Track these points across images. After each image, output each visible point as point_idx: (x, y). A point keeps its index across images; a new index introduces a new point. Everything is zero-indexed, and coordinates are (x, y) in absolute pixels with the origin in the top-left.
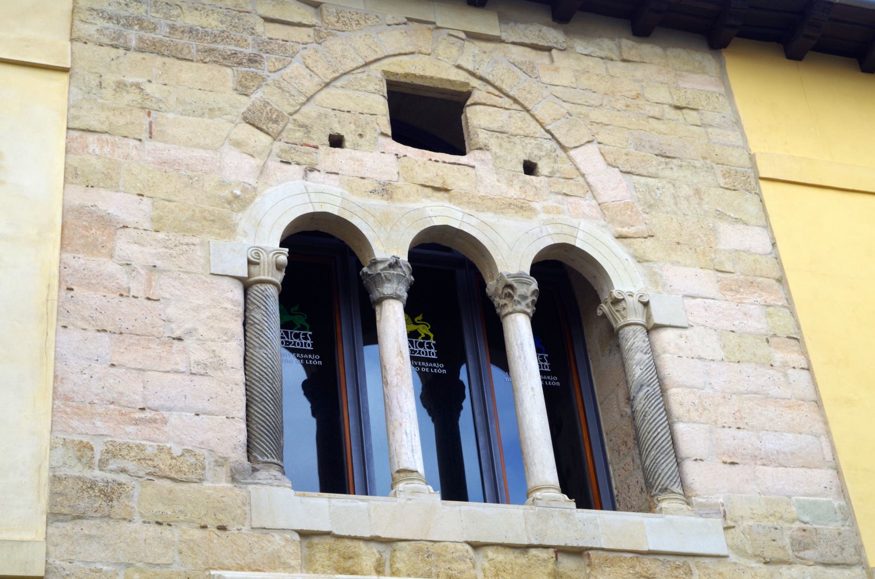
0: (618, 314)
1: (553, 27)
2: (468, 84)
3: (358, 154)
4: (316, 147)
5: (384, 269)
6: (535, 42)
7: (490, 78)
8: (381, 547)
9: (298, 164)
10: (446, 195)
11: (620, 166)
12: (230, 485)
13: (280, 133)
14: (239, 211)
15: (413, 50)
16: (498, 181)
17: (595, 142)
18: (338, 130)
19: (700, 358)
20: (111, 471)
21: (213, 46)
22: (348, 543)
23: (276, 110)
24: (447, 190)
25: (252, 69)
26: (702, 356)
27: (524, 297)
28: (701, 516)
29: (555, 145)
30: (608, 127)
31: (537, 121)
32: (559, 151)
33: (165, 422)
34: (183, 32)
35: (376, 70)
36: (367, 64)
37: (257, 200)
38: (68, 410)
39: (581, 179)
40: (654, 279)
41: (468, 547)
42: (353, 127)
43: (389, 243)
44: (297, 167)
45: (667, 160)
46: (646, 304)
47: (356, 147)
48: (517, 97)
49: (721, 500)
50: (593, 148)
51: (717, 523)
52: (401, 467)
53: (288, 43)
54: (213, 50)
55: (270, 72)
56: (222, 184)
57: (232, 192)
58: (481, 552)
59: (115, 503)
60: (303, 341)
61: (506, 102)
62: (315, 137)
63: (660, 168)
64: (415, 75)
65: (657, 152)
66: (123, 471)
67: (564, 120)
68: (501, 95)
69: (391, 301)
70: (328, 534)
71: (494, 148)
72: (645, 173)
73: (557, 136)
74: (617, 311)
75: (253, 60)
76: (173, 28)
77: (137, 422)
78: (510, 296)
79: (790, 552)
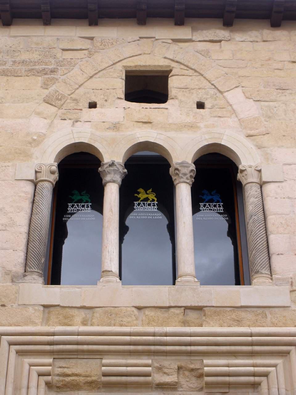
0: (243, 178)
1: (224, 29)
2: (170, 66)
3: (103, 110)
4: (81, 110)
5: (107, 168)
6: (212, 39)
7: (182, 61)
8: (87, 311)
9: (70, 119)
10: (150, 125)
11: (253, 98)
12: (11, 284)
13: (62, 105)
14: (35, 146)
15: (141, 53)
16: (181, 114)
17: (240, 87)
18: (94, 99)
19: (289, 198)
21: (33, 67)
22: (67, 310)
24: (150, 123)
25: (52, 76)
26: (290, 196)
27: (185, 174)
28: (277, 285)
30: (249, 78)
31: (207, 80)
32: (219, 94)
34: (19, 63)
35: (119, 66)
36: (114, 64)
37: (45, 140)
39: (230, 108)
41: (134, 309)
42: (102, 96)
43: (113, 155)
44: (70, 121)
45: (284, 91)
46: (260, 171)
47: (102, 106)
48: (196, 69)
49: (291, 276)
50: (239, 90)
51: (288, 288)
52: (104, 270)
53: (73, 60)
54: (33, 69)
55: (61, 76)
56: (28, 134)
57: (32, 138)
58: (143, 311)
60: (218, 208)
61: (190, 72)
62: (81, 104)
63: (279, 96)
64: (141, 66)
65: (277, 88)
67: (222, 77)
68: (188, 69)
69: (110, 184)
70: (58, 306)
71: (180, 98)
72: (268, 100)
73: (217, 86)
74: (243, 176)
75: (53, 71)
76: (14, 62)
78: (177, 174)
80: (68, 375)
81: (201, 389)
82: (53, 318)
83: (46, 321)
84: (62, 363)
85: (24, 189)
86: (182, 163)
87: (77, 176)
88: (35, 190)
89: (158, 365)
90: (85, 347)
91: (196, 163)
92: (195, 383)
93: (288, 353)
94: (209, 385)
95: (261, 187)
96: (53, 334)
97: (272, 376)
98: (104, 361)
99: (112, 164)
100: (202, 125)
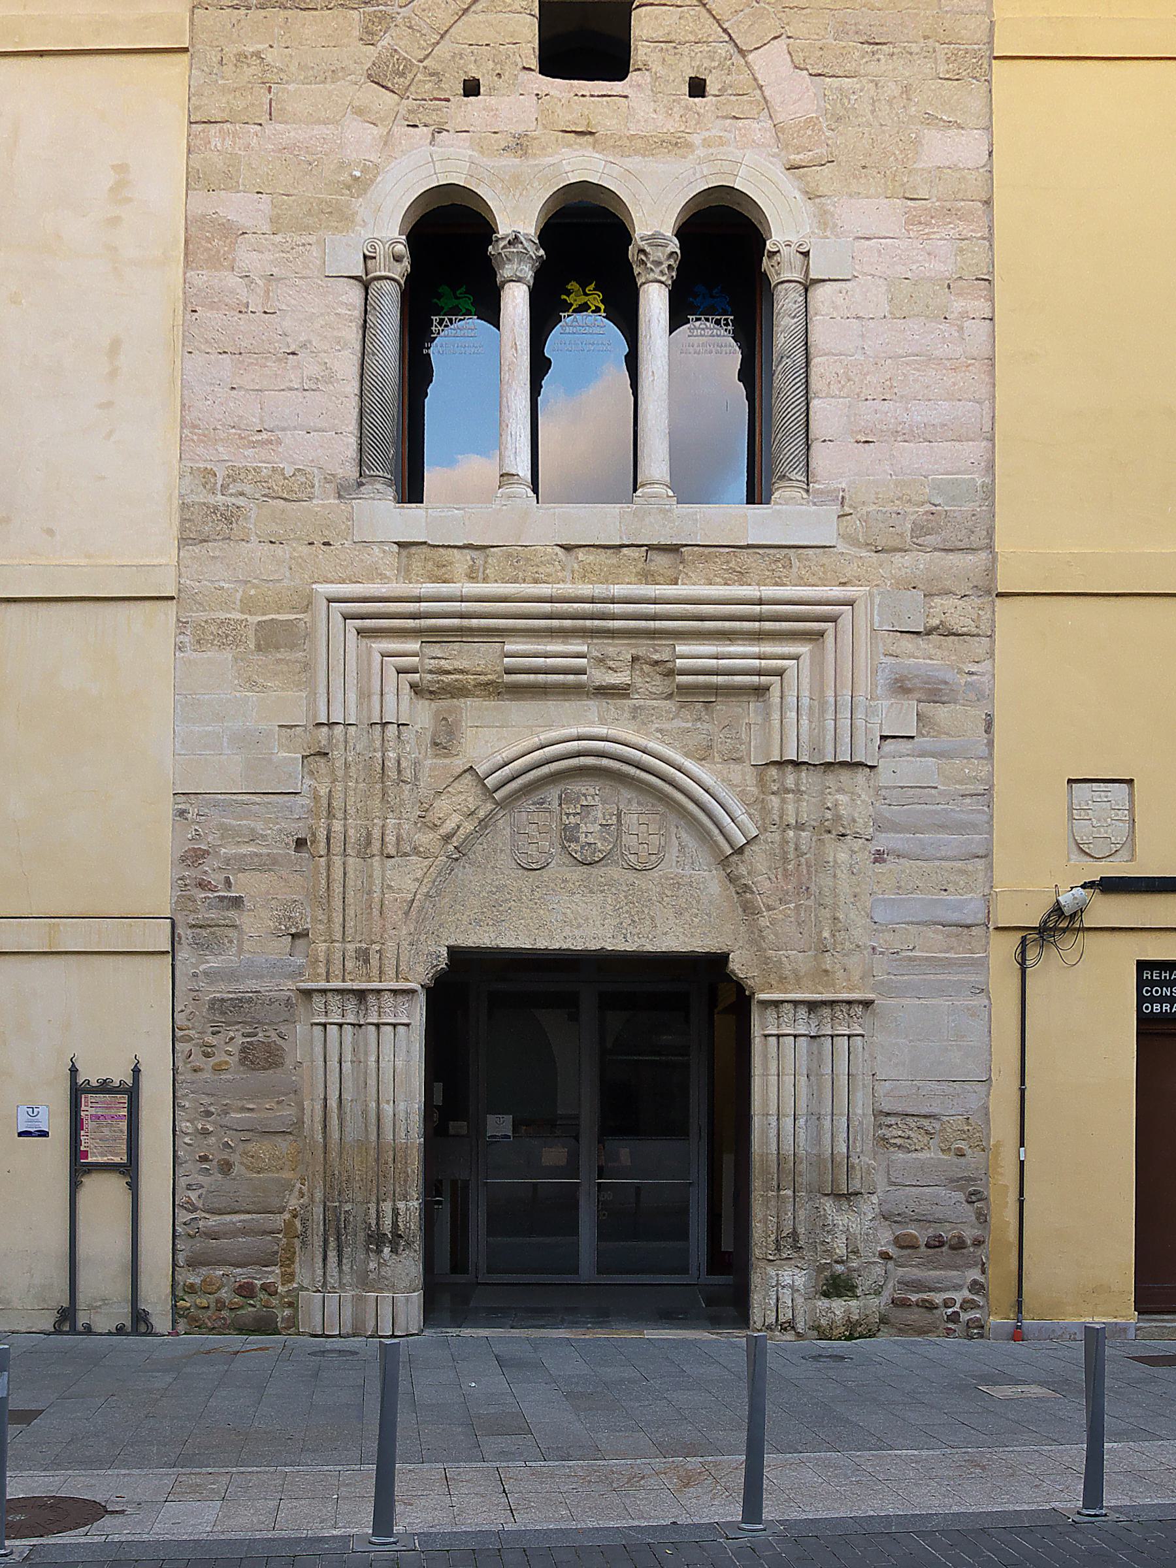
3: (492, 101)
4: (448, 100)
5: (504, 247)
8: (475, 554)
20: (231, 495)
23: (405, 58)
27: (658, 263)
28: (815, 504)
29: (733, 50)
33: (279, 442)
38: (195, 438)
40: (824, 220)
46: (806, 254)
47: (492, 91)
49: (844, 485)
51: (835, 509)
59: (234, 525)
66: (242, 494)
67: (747, 10)
71: (656, 67)
72: (840, 74)
77: (253, 445)
79: (908, 539)
80: (449, 673)
81: (670, 696)
82: (416, 566)
83: (405, 573)
84: (436, 650)
85: (344, 298)
86: (653, 237)
87: (448, 253)
88: (366, 299)
89: (596, 654)
90: (474, 622)
91: (679, 234)
92: (659, 684)
93: (821, 634)
94: (683, 689)
95: (806, 290)
96: (419, 600)
97: (790, 676)
98: (507, 647)
99: (515, 241)
100: (696, 139)
